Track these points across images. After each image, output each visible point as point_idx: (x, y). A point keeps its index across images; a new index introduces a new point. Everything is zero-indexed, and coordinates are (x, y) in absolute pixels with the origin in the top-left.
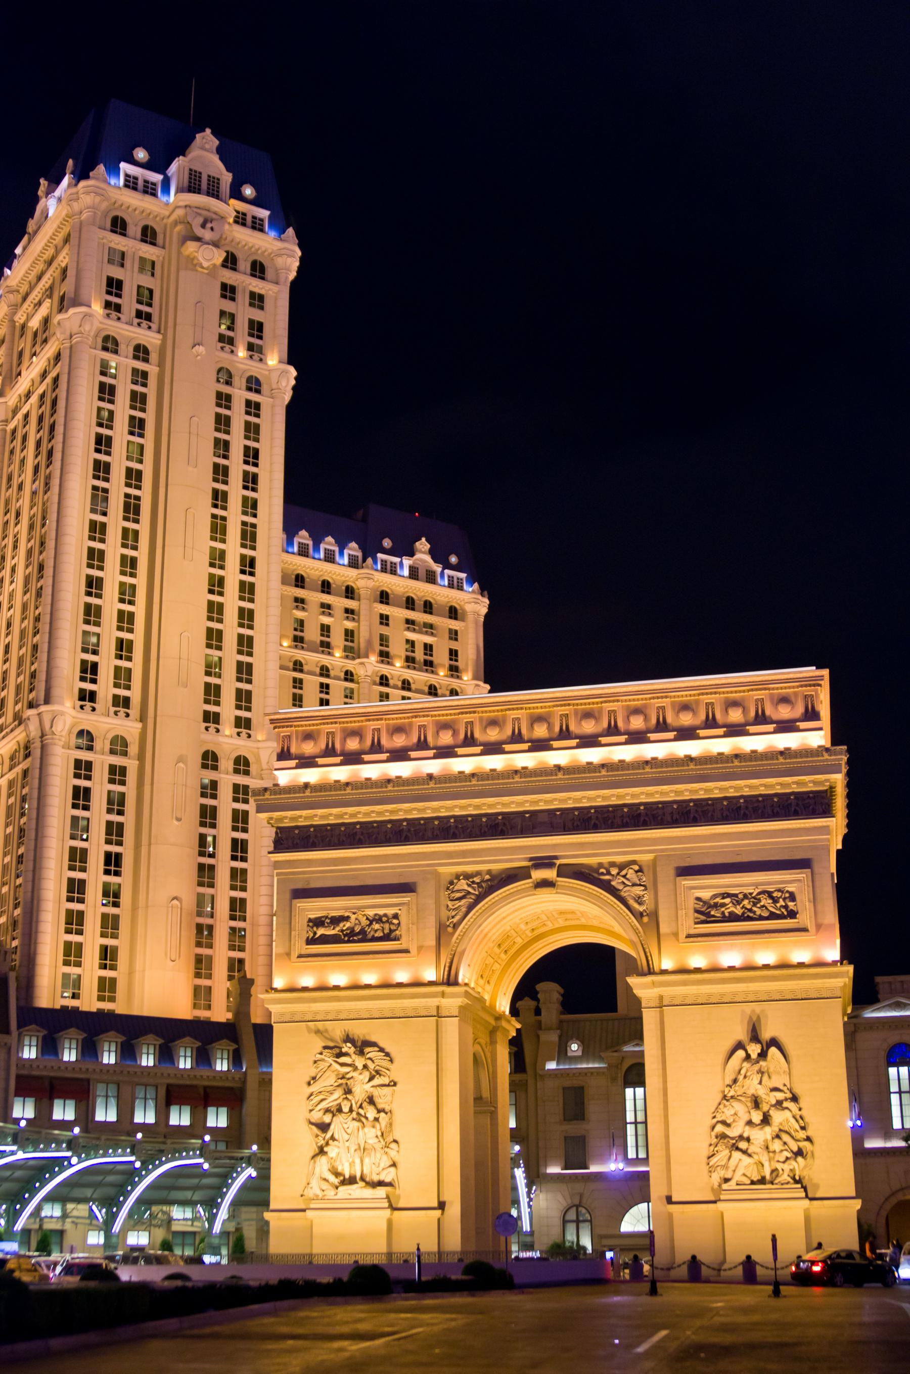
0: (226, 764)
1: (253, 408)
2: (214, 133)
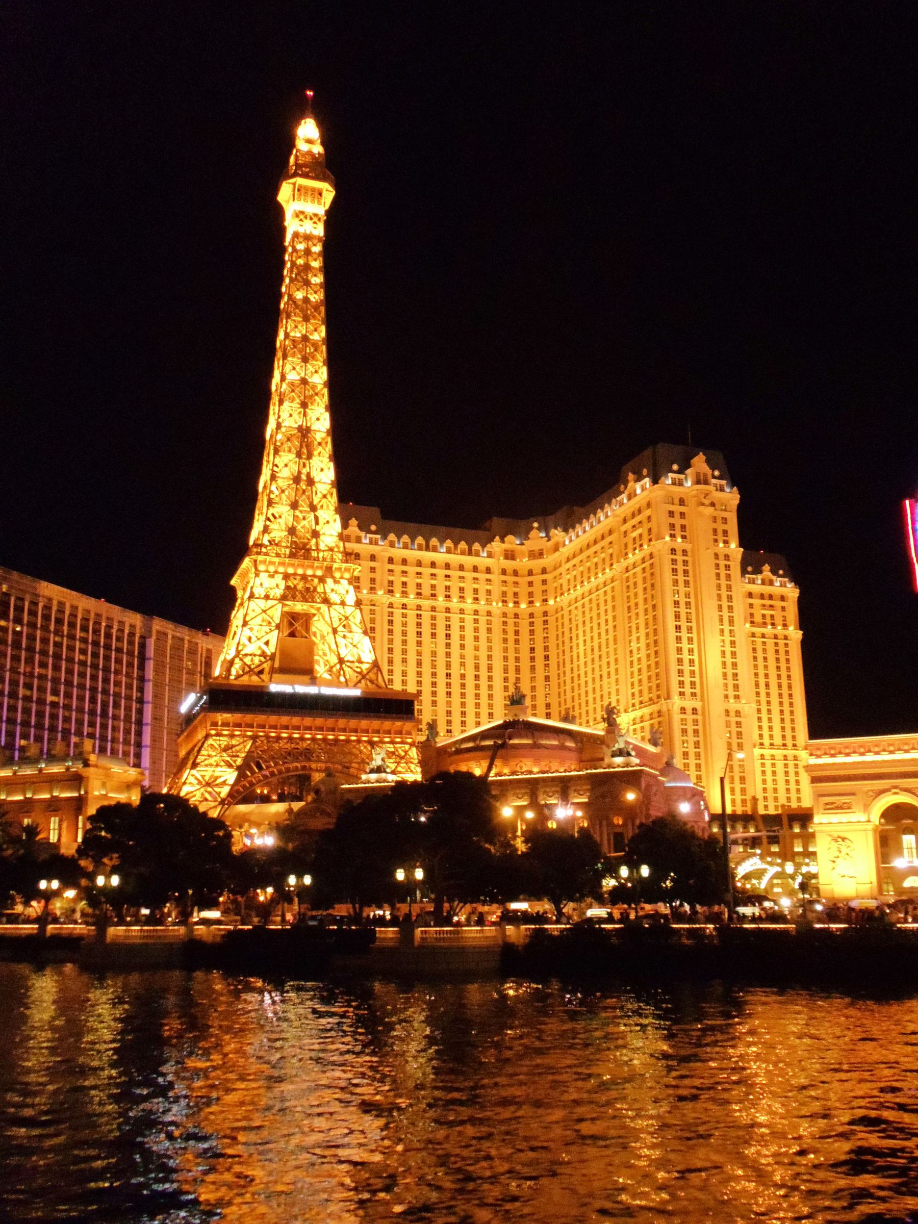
0: (732, 714)
1: (727, 567)
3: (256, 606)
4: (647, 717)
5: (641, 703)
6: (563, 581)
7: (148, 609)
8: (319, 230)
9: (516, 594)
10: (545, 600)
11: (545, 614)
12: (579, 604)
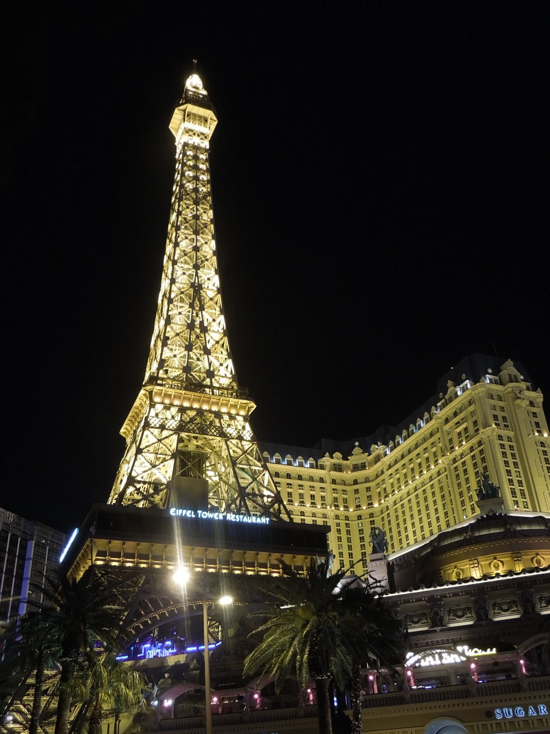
2: (511, 360)
3: (149, 438)
8: (206, 144)
9: (345, 501)
10: (370, 504)
11: (371, 515)
12: (405, 501)
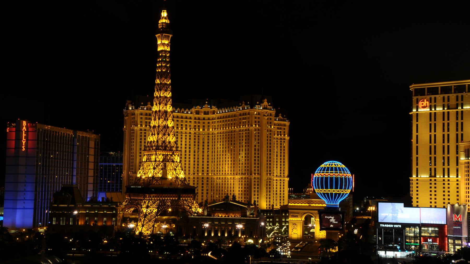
4: (243, 178)
5: (242, 173)
6: (216, 124)
7: (75, 128)
8: (169, 49)
9: (199, 126)
